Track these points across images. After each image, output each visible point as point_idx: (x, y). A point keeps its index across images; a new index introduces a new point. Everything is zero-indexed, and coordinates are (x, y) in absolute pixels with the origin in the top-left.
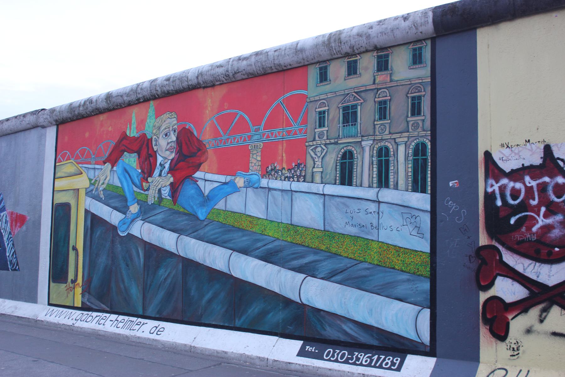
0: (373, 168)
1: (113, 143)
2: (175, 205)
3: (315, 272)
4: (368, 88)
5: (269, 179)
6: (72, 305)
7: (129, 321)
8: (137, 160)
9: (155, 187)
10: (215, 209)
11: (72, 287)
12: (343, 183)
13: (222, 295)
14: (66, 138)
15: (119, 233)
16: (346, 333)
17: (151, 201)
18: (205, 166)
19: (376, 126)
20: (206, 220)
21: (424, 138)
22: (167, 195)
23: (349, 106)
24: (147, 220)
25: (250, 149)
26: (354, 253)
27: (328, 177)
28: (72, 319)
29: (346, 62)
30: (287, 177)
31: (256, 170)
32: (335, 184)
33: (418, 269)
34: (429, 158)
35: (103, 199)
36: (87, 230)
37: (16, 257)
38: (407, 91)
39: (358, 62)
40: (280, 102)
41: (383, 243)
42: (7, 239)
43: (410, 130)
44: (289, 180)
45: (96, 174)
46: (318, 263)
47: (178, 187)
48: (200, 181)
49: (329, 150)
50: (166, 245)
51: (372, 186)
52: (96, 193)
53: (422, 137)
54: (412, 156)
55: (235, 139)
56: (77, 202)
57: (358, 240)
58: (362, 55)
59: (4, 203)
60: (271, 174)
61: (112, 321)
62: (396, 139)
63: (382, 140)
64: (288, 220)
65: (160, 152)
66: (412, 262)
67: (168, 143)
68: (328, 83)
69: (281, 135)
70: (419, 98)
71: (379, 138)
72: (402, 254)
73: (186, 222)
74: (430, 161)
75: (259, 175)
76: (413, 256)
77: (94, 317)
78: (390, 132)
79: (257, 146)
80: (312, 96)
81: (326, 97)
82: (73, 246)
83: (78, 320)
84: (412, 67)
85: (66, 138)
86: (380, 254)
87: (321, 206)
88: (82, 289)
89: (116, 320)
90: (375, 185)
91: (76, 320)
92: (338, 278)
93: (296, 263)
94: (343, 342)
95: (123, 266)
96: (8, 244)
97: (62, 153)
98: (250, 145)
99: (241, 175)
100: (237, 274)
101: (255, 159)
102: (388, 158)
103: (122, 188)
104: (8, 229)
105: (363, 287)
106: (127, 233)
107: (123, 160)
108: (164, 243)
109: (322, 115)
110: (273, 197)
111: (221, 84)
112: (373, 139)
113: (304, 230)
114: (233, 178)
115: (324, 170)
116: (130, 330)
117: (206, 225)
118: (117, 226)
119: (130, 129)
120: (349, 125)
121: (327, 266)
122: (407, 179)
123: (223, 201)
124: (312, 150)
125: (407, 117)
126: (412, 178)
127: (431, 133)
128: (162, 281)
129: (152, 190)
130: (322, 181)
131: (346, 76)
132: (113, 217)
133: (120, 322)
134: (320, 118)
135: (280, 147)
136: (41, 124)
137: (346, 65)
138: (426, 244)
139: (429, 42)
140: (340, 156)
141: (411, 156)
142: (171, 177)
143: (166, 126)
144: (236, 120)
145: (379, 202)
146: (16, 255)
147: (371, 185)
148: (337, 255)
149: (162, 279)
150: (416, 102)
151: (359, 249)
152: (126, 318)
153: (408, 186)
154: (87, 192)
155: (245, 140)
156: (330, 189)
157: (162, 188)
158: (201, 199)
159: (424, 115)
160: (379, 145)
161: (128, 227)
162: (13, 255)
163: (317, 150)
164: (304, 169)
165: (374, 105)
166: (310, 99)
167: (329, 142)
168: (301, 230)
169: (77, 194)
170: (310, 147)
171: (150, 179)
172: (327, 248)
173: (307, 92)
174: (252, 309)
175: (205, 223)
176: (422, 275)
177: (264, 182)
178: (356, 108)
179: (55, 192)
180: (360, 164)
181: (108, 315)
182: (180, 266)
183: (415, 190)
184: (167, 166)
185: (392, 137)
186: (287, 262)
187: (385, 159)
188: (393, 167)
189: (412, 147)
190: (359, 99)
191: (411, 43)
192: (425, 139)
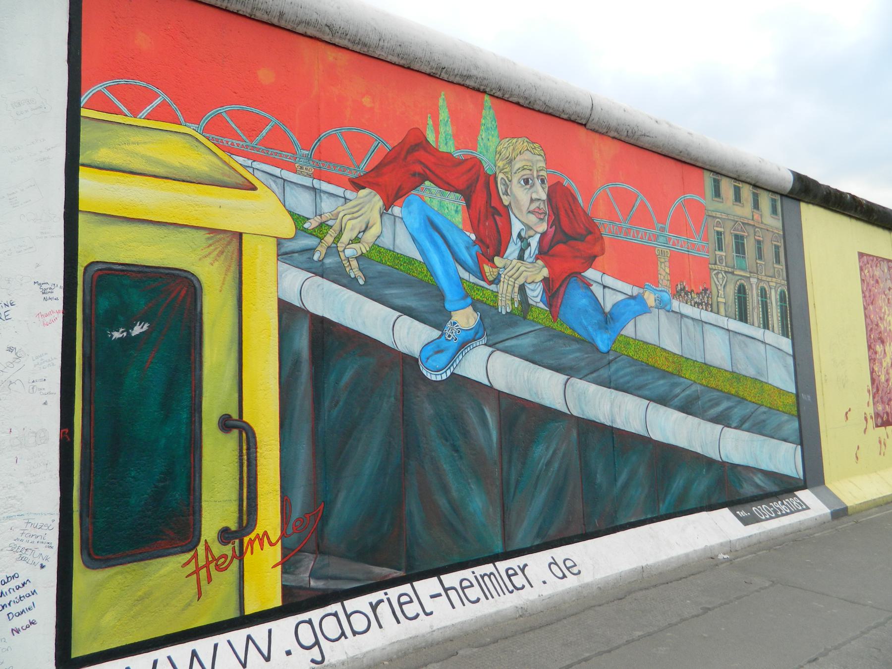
2: (555, 320)
5: (680, 301)
9: (511, 279)
10: (622, 335)
12: (741, 320)
13: (642, 471)
15: (424, 372)
16: (758, 486)
17: (505, 307)
22: (538, 299)
24: (500, 346)
27: (730, 310)
31: (666, 286)
32: (735, 319)
35: (361, 282)
36: (297, 363)
48: (594, 285)
50: (544, 396)
52: (328, 261)
53: (783, 285)
60: (681, 295)
65: (516, 212)
73: (578, 354)
79: (664, 251)
92: (746, 425)
93: (713, 412)
95: (442, 452)
98: (657, 249)
99: (651, 289)
100: (656, 436)
101: (664, 270)
103: (427, 263)
106: (449, 373)
107: (421, 197)
108: (540, 393)
114: (641, 291)
118: (417, 355)
121: (738, 413)
123: (632, 323)
124: (715, 275)
128: (541, 471)
130: (726, 315)
142: (543, 267)
143: (524, 163)
152: (467, 573)
157: (528, 286)
161: (453, 358)
171: (497, 260)
177: (676, 304)
180: (751, 301)
182: (574, 434)
183: (783, 335)
184: (534, 242)
185: (767, 280)
186: (705, 411)
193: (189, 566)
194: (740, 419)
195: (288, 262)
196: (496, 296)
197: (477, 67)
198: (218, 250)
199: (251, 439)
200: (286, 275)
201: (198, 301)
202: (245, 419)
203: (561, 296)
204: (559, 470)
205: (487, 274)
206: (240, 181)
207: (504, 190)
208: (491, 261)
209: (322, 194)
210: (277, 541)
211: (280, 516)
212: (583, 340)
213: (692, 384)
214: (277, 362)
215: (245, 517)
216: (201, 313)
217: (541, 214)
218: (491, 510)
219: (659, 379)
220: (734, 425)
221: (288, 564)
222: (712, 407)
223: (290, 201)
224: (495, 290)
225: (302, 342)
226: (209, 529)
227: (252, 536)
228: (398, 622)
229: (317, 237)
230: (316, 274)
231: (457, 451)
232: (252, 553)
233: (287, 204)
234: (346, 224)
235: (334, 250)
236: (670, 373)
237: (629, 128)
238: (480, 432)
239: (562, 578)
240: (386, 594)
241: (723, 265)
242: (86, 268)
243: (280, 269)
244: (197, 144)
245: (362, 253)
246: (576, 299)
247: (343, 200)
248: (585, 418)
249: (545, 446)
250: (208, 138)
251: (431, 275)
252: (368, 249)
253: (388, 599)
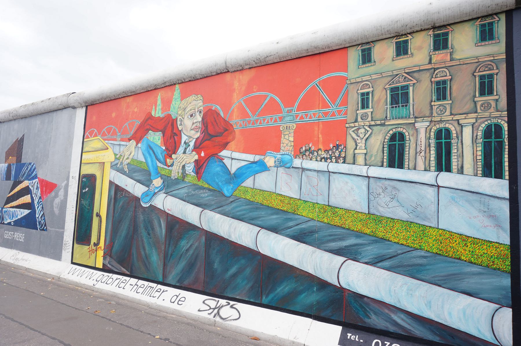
0: (430, 150)
1: (138, 123)
2: (199, 180)
3: (356, 256)
4: (422, 68)
5: (303, 159)
6: (94, 266)
7: (149, 287)
8: (161, 138)
9: (179, 163)
10: (242, 186)
11: (95, 249)
12: (391, 165)
13: (248, 271)
14: (94, 118)
15: (142, 204)
16: (396, 324)
18: (232, 144)
19: (433, 107)
20: (232, 197)
21: (498, 119)
22: (191, 171)
23: (399, 87)
25: (281, 129)
26: (406, 239)
27: (373, 158)
28: (93, 280)
29: (395, 43)
30: (324, 158)
31: (289, 150)
32: (382, 166)
33: (493, 262)
34: (506, 141)
35: (127, 172)
36: (111, 199)
37: (44, 219)
38: (474, 69)
39: (410, 42)
40: (316, 84)
41: (444, 230)
42: (38, 202)
43: (479, 111)
44: (326, 161)
45: (122, 149)
46: (361, 247)
47: (203, 164)
49: (373, 131)
51: (429, 169)
53: (496, 117)
54: (482, 138)
55: (264, 120)
56: (102, 174)
57: (412, 226)
58: (414, 35)
59: (36, 172)
60: (305, 155)
61: (132, 285)
62: (460, 120)
63: (441, 121)
64: (325, 201)
65: (184, 131)
66: (484, 253)
67: (193, 124)
68: (372, 64)
69: (317, 116)
70: (491, 76)
71: (438, 119)
72: (471, 244)
73: (211, 198)
74: (507, 144)
75: (291, 155)
76: (485, 247)
77: (114, 279)
78: (451, 113)
79: (289, 127)
80: (353, 77)
81: (370, 78)
82: (97, 213)
83: (99, 281)
84: (479, 44)
85: (94, 118)
86: (441, 243)
87: (365, 188)
88: (104, 252)
89: (136, 285)
90: (433, 169)
91: (96, 281)
92: (386, 264)
93: (334, 245)
94: (392, 333)
95: (144, 233)
96: (38, 207)
97: (90, 130)
102: (450, 140)
104: (39, 194)
105: (419, 276)
106: (149, 204)
107: (147, 138)
109: (365, 97)
110: (308, 177)
111: (250, 68)
112: (430, 120)
113: (344, 212)
114: (262, 157)
115: (368, 151)
116: (150, 296)
117: (232, 202)
119: (156, 110)
120: (399, 106)
121: (373, 250)
122: (475, 163)
123: (252, 178)
124: (353, 131)
125: (475, 96)
126: (483, 162)
127: (508, 114)
128: (183, 252)
129: (176, 166)
131: (395, 57)
132: (136, 189)
133: (140, 287)
134: (363, 100)
135: (316, 129)
136: (72, 105)
137: (395, 45)
138: (504, 234)
139: (503, 17)
140: (387, 138)
141: (481, 139)
143: (191, 107)
144: (266, 102)
145: (439, 187)
146: (44, 217)
147: (428, 168)
148: (385, 239)
149: (183, 250)
150: (486, 80)
151: (413, 235)
152: (146, 283)
153: (477, 170)
154: (112, 165)
155: (276, 121)
156: (375, 172)
158: (227, 177)
159: (497, 95)
160: (438, 127)
161: (151, 199)
162: (42, 217)
163: (360, 131)
164: (344, 150)
165: (430, 85)
166: (350, 81)
167: (374, 124)
168: (341, 212)
169: (103, 167)
170: (351, 128)
172: (372, 232)
173: (347, 74)
174: (282, 287)
175: (231, 200)
176: (499, 269)
177: (297, 162)
178: (408, 89)
179: (82, 164)
181: (128, 278)
182: (203, 239)
184: (192, 144)
186: (323, 243)
187: (445, 142)
188: (456, 150)
189: (482, 129)
190: (411, 80)
191: (478, 18)
192: (499, 121)
194: (374, 256)
197: (166, 78)
203: (204, 168)
204: (193, 253)
205: (168, 163)
207: (180, 123)
208: (170, 157)
212: (215, 190)
213: (309, 221)
218: (159, 262)
219: (272, 214)
222: (334, 240)
231: (149, 235)
236: (285, 211)
237: (253, 59)
238: (157, 229)
239: (171, 302)
241: (368, 120)
246: (214, 168)
248: (211, 232)
249: (187, 242)
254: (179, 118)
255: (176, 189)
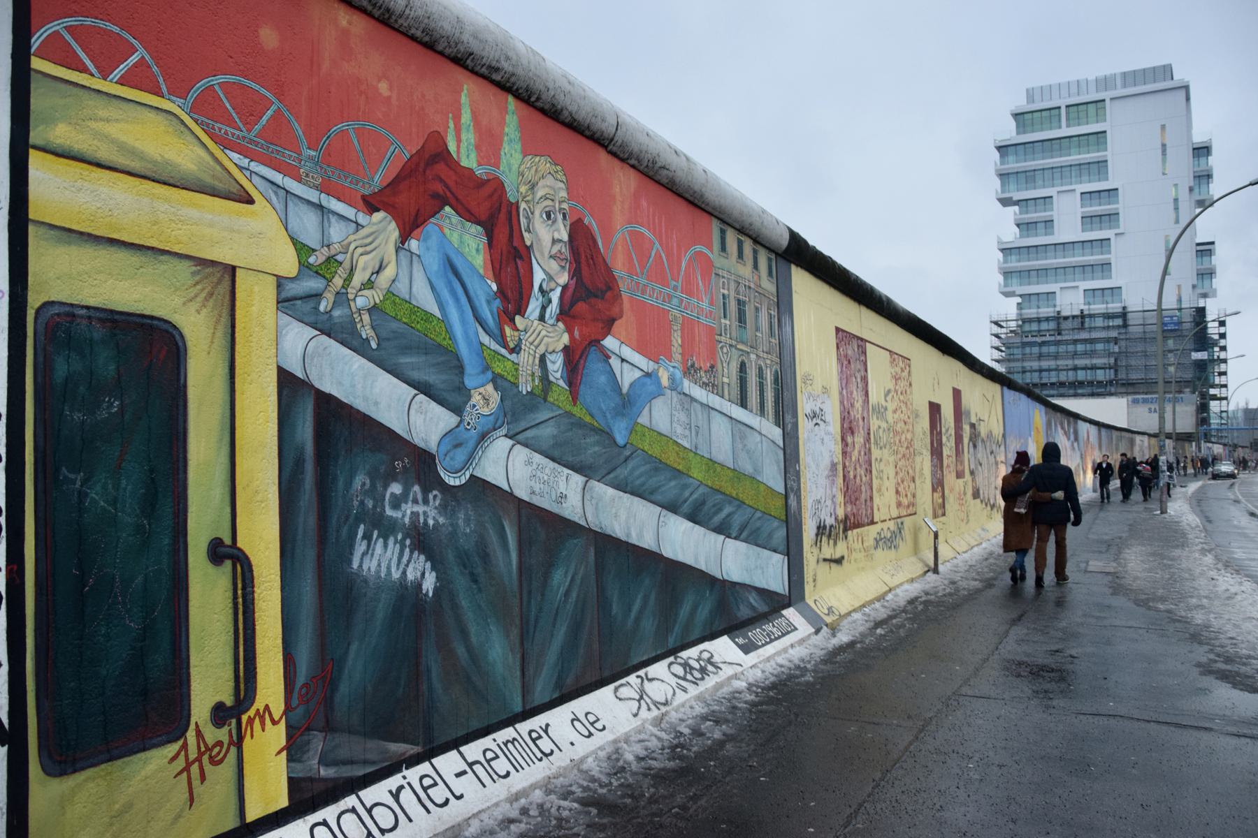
2: (575, 404)
8: (484, 248)
9: (532, 347)
15: (442, 475)
22: (558, 375)
24: (520, 437)
35: (374, 345)
36: (299, 462)
47: (578, 361)
48: (613, 357)
52: (336, 313)
73: (596, 449)
92: (744, 534)
100: (668, 552)
103: (445, 320)
106: (468, 476)
114: (656, 366)
143: (547, 190)
152: (486, 742)
171: (518, 318)
175: (627, 453)
177: (688, 386)
183: (776, 425)
184: (555, 296)
193: (176, 762)
195: (290, 313)
196: (517, 370)
198: (206, 291)
199: (247, 574)
200: (287, 332)
201: (182, 367)
202: (240, 544)
204: (578, 596)
206: (234, 189)
207: (526, 225)
209: (331, 216)
210: (281, 718)
211: (282, 682)
212: (601, 430)
214: (276, 461)
215: (242, 686)
216: (185, 386)
217: (562, 260)
220: (734, 535)
221: (294, 749)
222: (716, 513)
223: (293, 223)
224: (516, 361)
225: (305, 431)
226: (200, 710)
227: (252, 712)
228: (428, 811)
229: (324, 277)
230: (323, 332)
231: (475, 581)
232: (252, 736)
233: (290, 227)
234: (357, 262)
235: (344, 297)
238: (500, 554)
239: (588, 737)
240: (404, 778)
242: (38, 311)
243: (280, 323)
244: (183, 128)
245: (376, 304)
247: (354, 225)
250: (196, 121)
251: (450, 339)
252: (382, 299)
253: (409, 784)
254: (523, 205)
255: (533, 424)
